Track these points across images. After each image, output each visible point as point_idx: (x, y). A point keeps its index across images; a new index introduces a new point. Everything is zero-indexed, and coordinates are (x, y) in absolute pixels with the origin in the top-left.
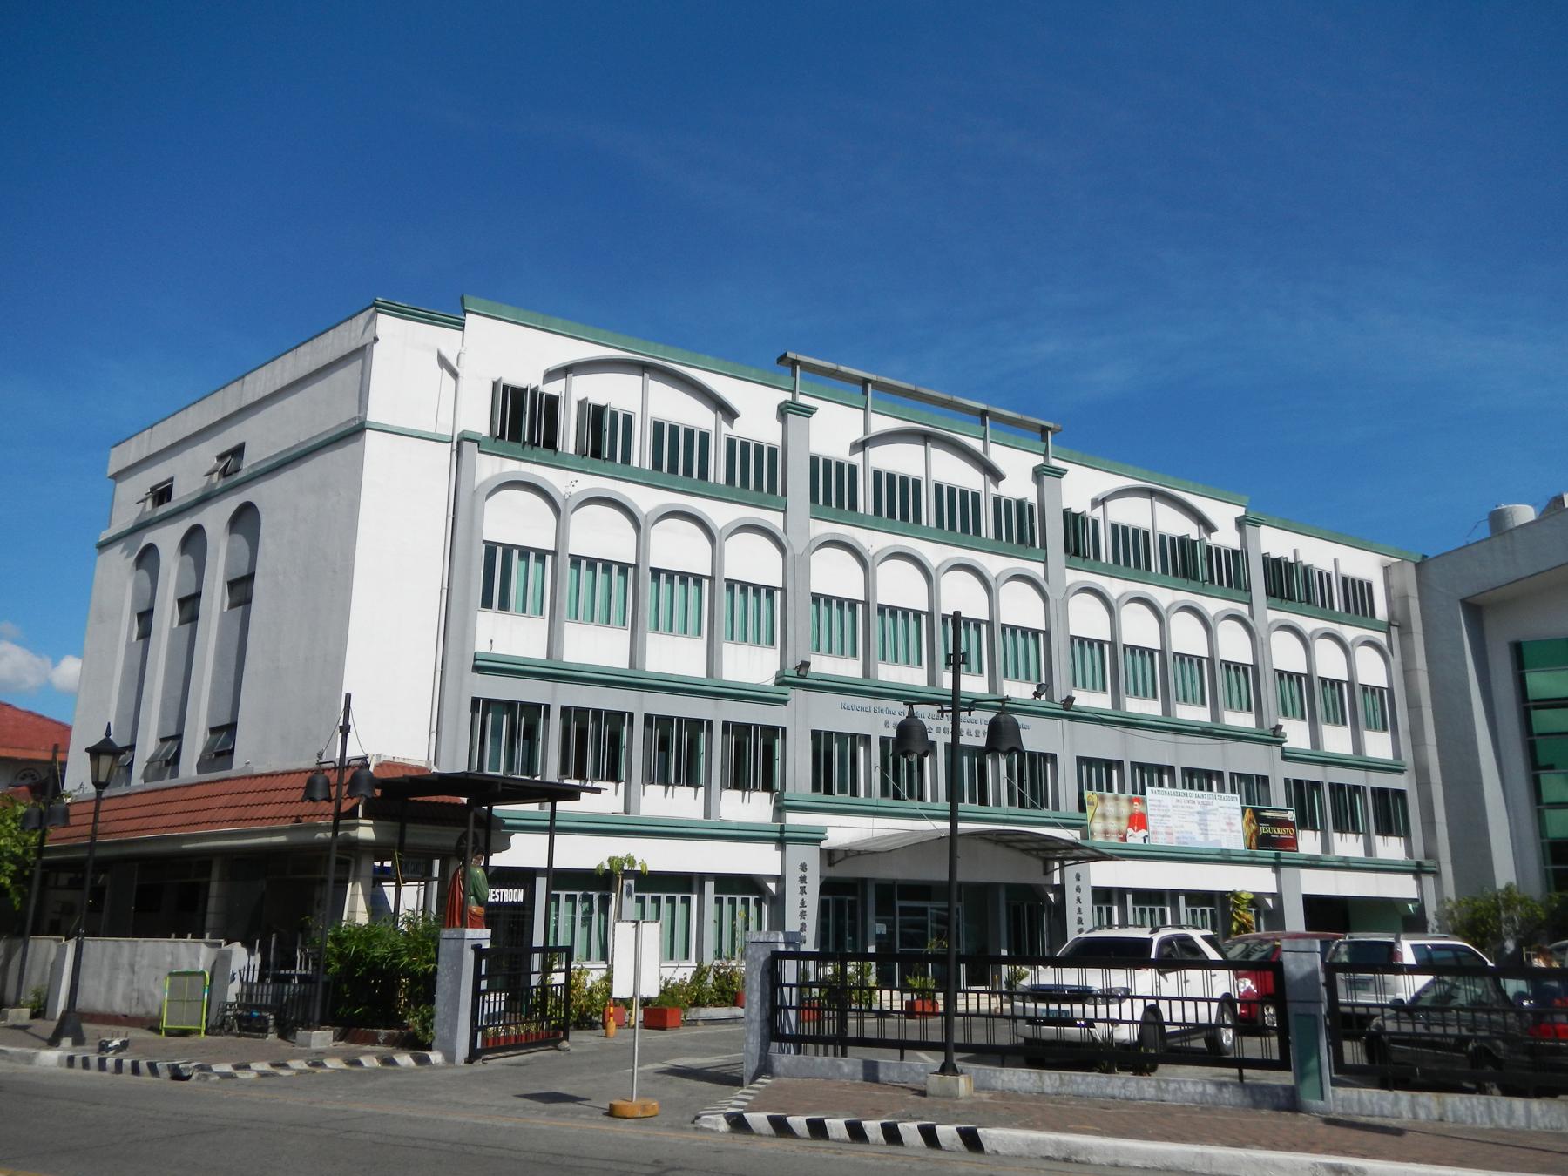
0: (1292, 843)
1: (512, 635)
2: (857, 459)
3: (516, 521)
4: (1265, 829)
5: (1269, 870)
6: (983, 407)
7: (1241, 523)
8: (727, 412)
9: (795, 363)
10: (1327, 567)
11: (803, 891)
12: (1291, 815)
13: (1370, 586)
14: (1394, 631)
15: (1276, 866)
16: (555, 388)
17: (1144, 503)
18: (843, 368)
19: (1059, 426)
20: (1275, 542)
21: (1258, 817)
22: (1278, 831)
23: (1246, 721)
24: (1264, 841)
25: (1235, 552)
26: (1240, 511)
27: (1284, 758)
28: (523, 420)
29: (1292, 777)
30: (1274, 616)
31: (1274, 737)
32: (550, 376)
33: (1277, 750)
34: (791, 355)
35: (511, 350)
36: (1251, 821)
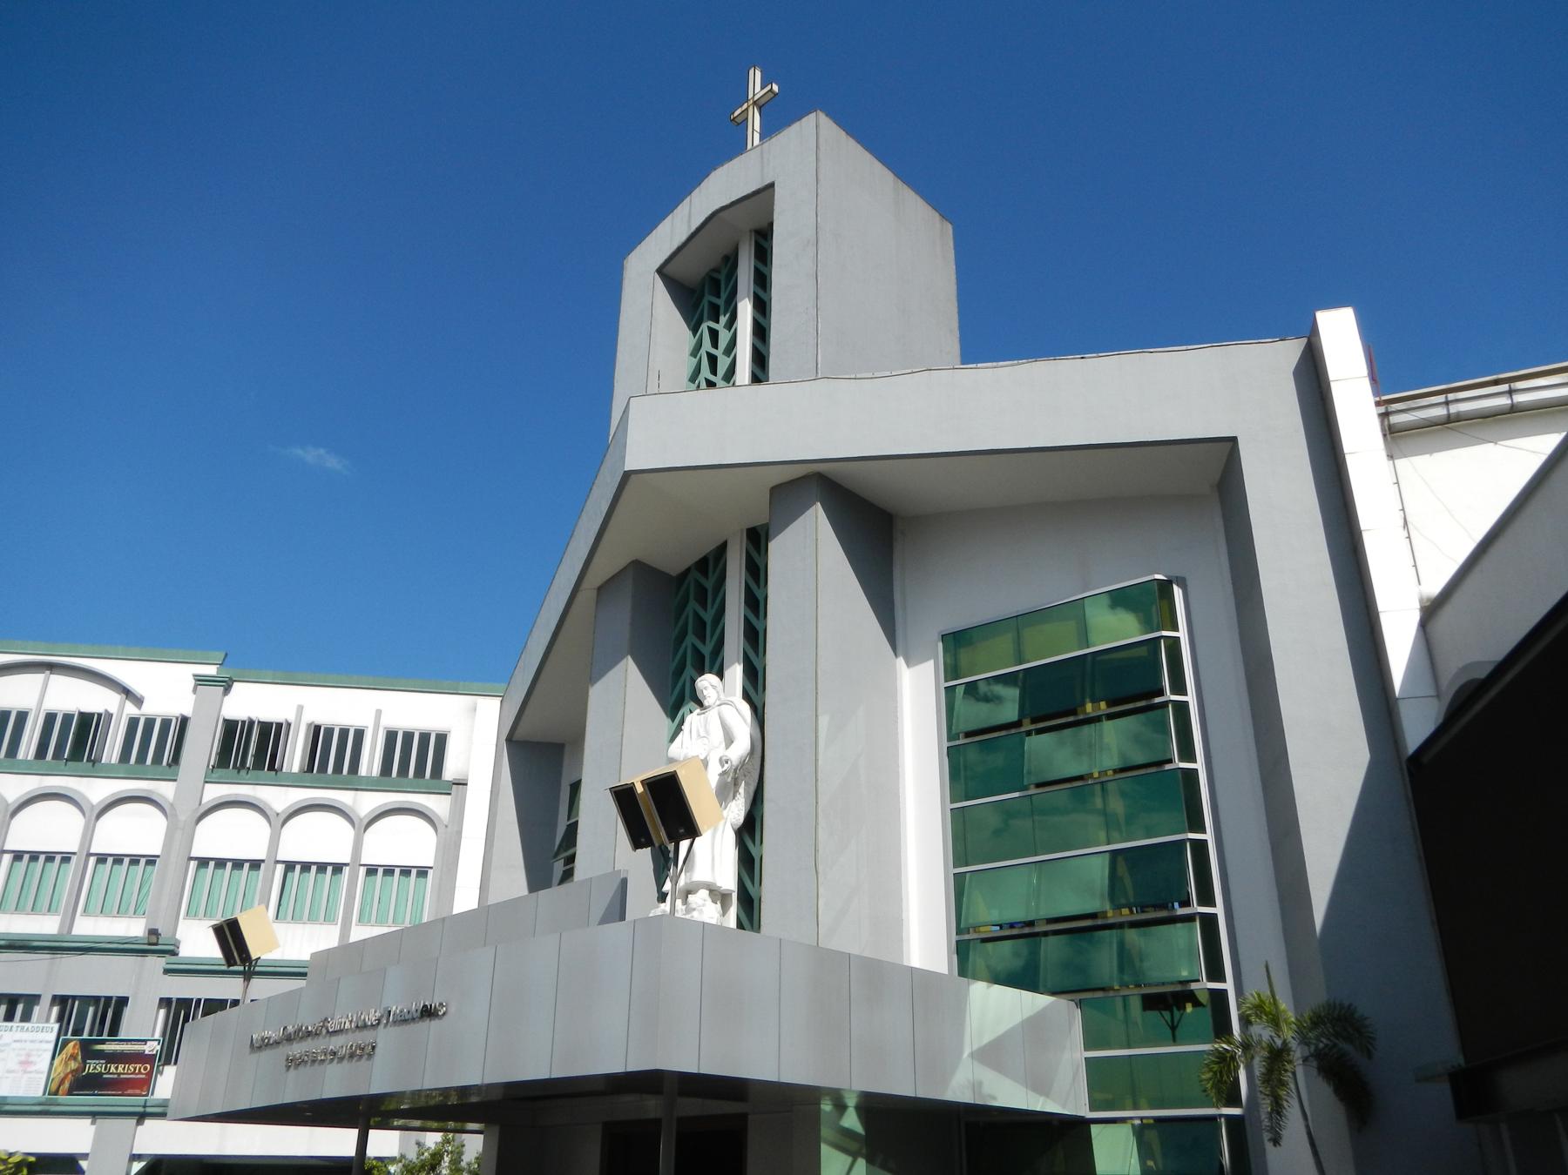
0: (146, 1084)
4: (94, 1067)
5: (87, 1122)
7: (201, 681)
12: (152, 1048)
13: (442, 739)
15: (94, 1115)
17: (38, 678)
21: (88, 1051)
22: (120, 1070)
23: (133, 928)
24: (84, 1083)
25: (184, 721)
26: (211, 670)
27: (167, 971)
29: (175, 994)
30: (214, 792)
31: (156, 945)
33: (157, 963)
36: (73, 1057)
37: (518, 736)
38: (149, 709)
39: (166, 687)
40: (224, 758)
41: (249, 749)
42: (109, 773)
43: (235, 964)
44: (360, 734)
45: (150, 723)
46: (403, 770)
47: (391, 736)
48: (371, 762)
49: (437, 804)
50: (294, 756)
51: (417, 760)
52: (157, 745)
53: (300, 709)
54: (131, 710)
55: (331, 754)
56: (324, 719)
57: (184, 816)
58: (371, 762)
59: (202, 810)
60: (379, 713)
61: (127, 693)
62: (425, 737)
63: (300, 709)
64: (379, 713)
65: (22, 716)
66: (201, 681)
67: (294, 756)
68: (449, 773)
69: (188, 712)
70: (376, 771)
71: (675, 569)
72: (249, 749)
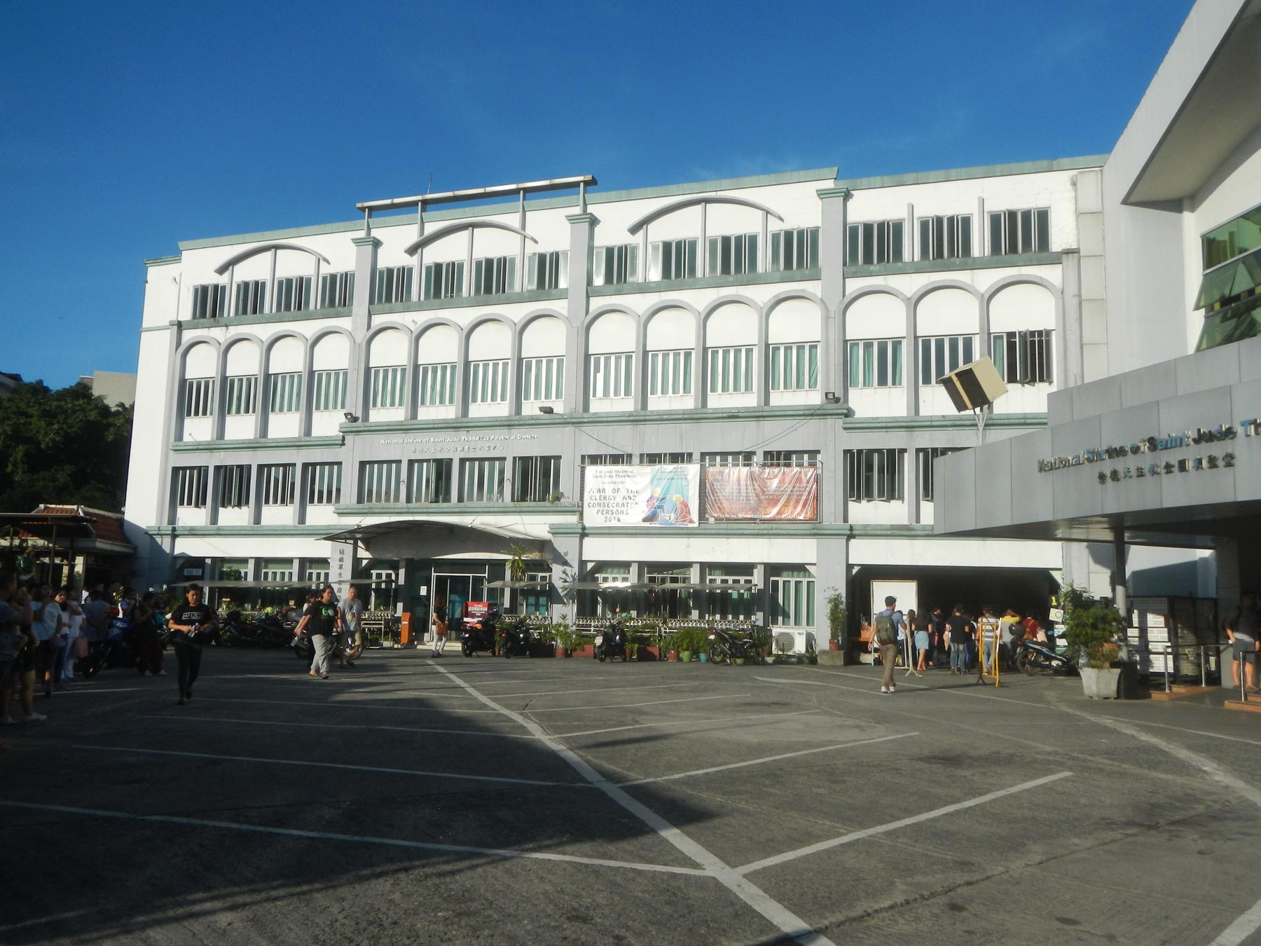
1: (199, 429)
2: (412, 261)
3: (202, 366)
6: (513, 187)
8: (320, 259)
9: (363, 209)
11: (341, 567)
13: (1043, 216)
16: (223, 280)
18: (397, 201)
19: (589, 178)
20: (875, 204)
25: (815, 233)
26: (829, 184)
28: (208, 304)
30: (854, 285)
32: (221, 271)
34: (359, 205)
35: (200, 264)
37: (1132, 199)
38: (787, 226)
39: (796, 202)
40: (850, 257)
41: (875, 247)
42: (765, 280)
43: (966, 408)
44: (966, 221)
45: (788, 235)
46: (1013, 249)
47: (995, 219)
48: (980, 243)
49: (1052, 273)
50: (911, 248)
51: (1021, 236)
52: (797, 252)
54: (775, 226)
55: (946, 242)
57: (834, 308)
58: (980, 243)
59: (847, 300)
62: (1027, 215)
66: (822, 194)
67: (911, 248)
68: (1056, 245)
69: (819, 224)
70: (988, 251)
72: (875, 247)
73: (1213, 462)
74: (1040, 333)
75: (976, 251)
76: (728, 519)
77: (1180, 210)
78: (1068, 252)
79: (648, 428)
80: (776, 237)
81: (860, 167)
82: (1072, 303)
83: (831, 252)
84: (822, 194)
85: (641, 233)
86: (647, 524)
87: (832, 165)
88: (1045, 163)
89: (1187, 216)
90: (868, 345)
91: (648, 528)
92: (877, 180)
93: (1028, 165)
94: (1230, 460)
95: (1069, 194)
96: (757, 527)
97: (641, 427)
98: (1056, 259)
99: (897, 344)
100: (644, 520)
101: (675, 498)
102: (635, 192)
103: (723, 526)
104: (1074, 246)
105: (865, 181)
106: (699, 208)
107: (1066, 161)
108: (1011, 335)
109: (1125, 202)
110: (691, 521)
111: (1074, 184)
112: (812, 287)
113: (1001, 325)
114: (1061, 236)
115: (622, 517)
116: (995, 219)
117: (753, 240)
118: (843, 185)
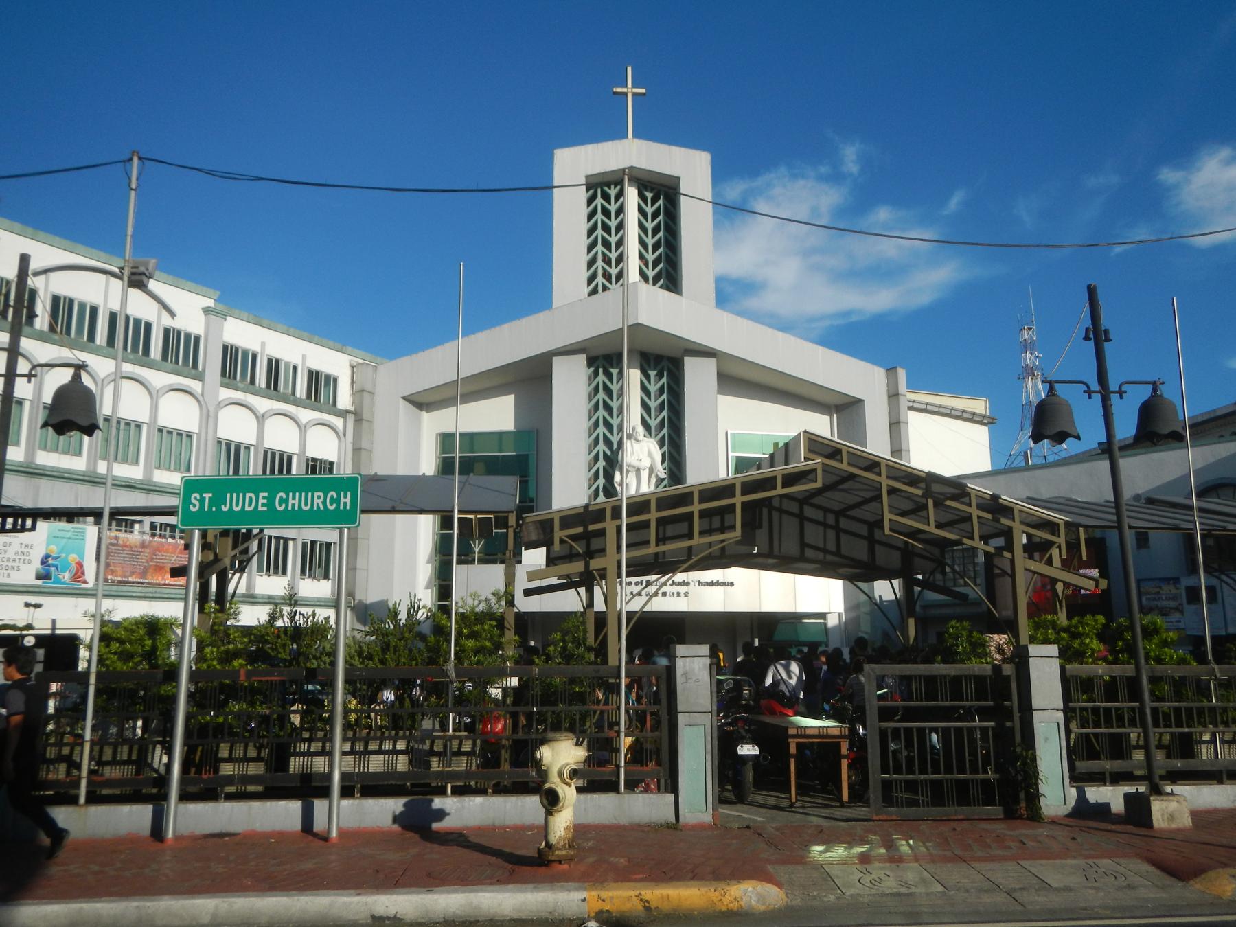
10: (297, 361)
13: (335, 380)
14: (350, 419)
26: (210, 303)
30: (226, 394)
41: (235, 365)
44: (295, 368)
49: (338, 422)
51: (319, 388)
53: (263, 344)
54: (167, 321)
56: (276, 354)
60: (304, 357)
61: (165, 307)
62: (328, 377)
63: (263, 344)
64: (304, 357)
65: (94, 310)
66: (207, 311)
70: (304, 396)
71: (593, 354)
73: (679, 594)
74: (332, 464)
75: (298, 394)
76: (119, 582)
77: (421, 409)
78: (350, 412)
79: (44, 483)
80: (167, 331)
81: (233, 300)
82: (350, 448)
83: (211, 361)
84: (207, 311)
85: (43, 277)
86: (40, 582)
87: (216, 289)
88: (339, 346)
89: (425, 416)
90: (228, 445)
91: (39, 587)
92: (245, 315)
93: (331, 343)
94: (686, 595)
95: (348, 372)
96: (144, 590)
97: (36, 481)
98: (343, 414)
99: (248, 448)
100: (38, 577)
101: (73, 558)
102: (42, 234)
103: (114, 588)
104: (352, 409)
105: (236, 312)
106: (103, 277)
107: (349, 349)
108: (314, 460)
109: (404, 398)
110: (85, 582)
111: (353, 367)
112: (195, 386)
113: (312, 452)
114: (344, 400)
115: (13, 574)
116: (310, 372)
117: (148, 326)
118: (221, 307)
